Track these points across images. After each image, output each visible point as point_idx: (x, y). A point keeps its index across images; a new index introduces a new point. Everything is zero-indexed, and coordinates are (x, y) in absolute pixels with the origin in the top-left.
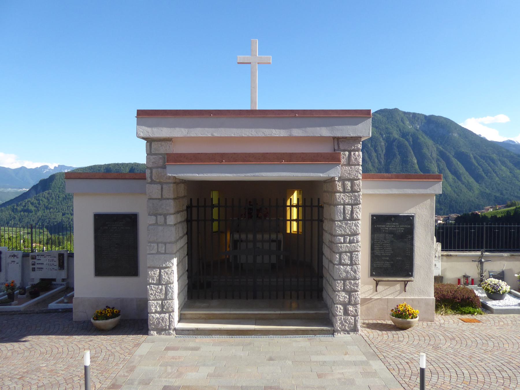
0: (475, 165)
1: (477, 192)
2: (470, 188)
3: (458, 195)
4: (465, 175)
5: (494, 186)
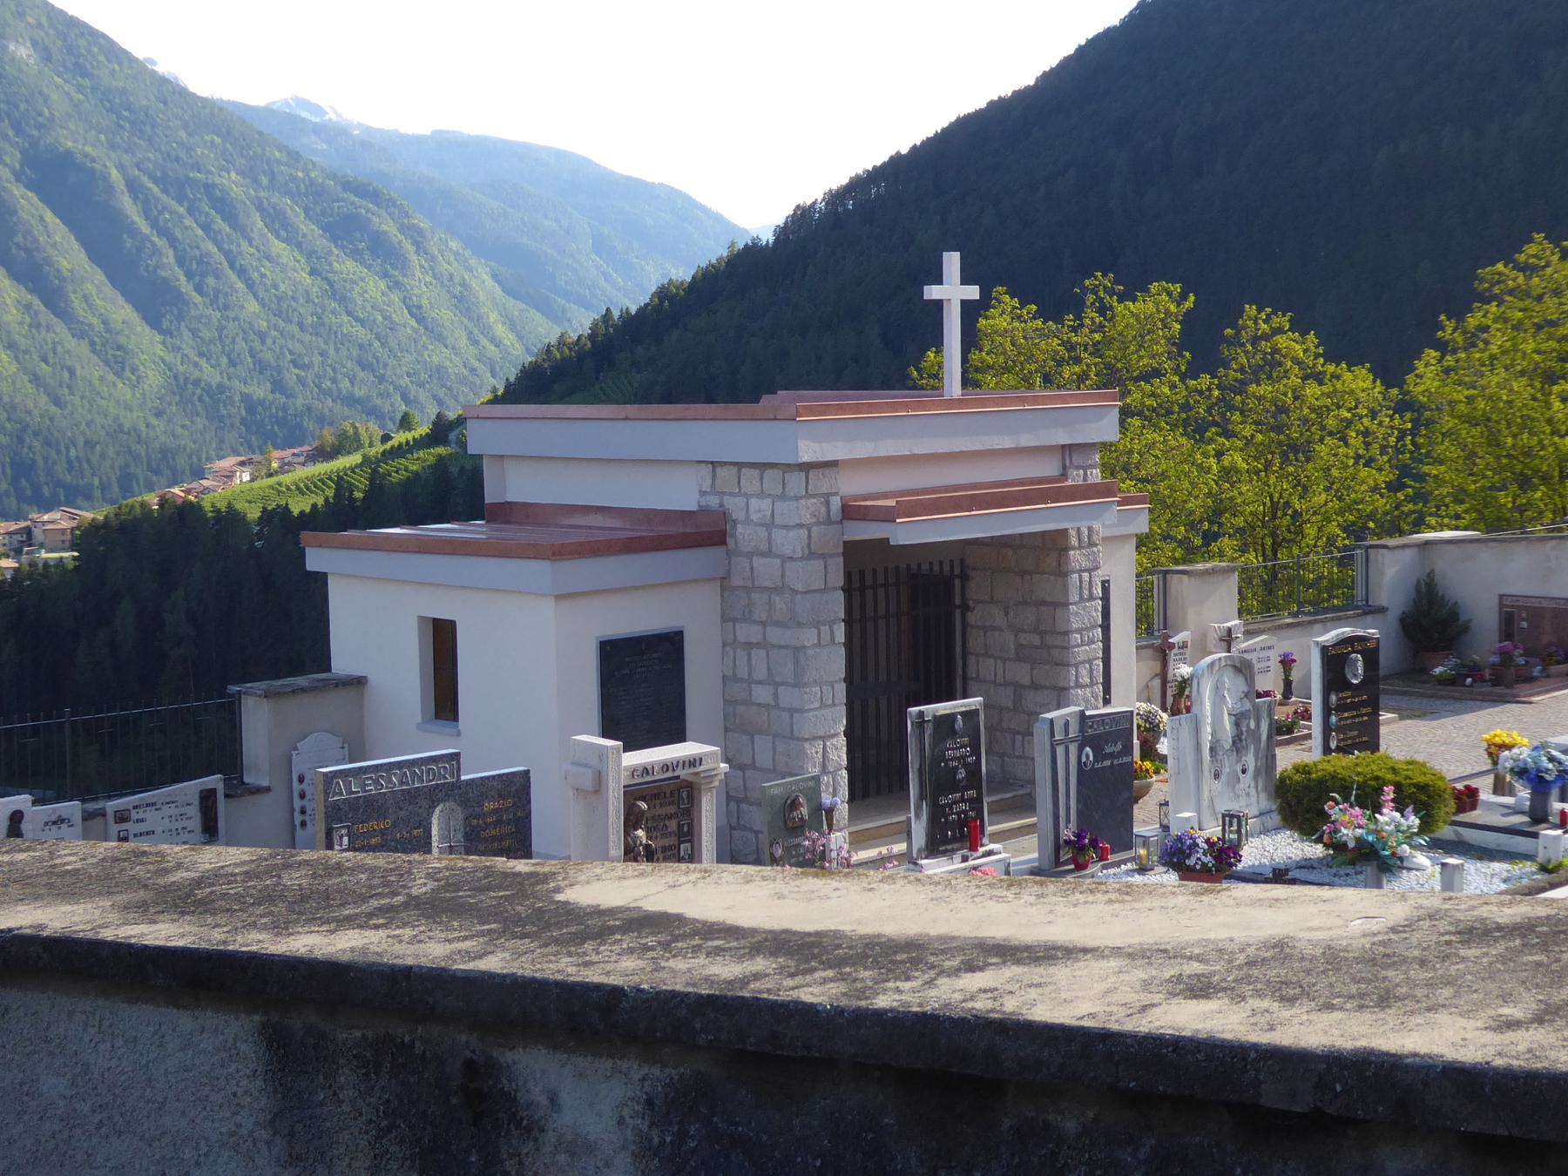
0: (133, 231)
1: (154, 380)
2: (118, 360)
3: (57, 402)
4: (90, 288)
5: (241, 345)
